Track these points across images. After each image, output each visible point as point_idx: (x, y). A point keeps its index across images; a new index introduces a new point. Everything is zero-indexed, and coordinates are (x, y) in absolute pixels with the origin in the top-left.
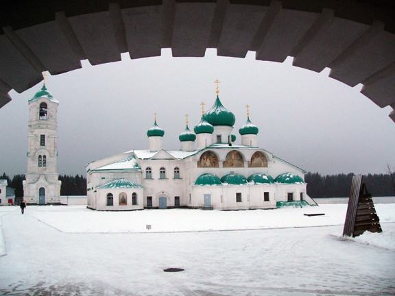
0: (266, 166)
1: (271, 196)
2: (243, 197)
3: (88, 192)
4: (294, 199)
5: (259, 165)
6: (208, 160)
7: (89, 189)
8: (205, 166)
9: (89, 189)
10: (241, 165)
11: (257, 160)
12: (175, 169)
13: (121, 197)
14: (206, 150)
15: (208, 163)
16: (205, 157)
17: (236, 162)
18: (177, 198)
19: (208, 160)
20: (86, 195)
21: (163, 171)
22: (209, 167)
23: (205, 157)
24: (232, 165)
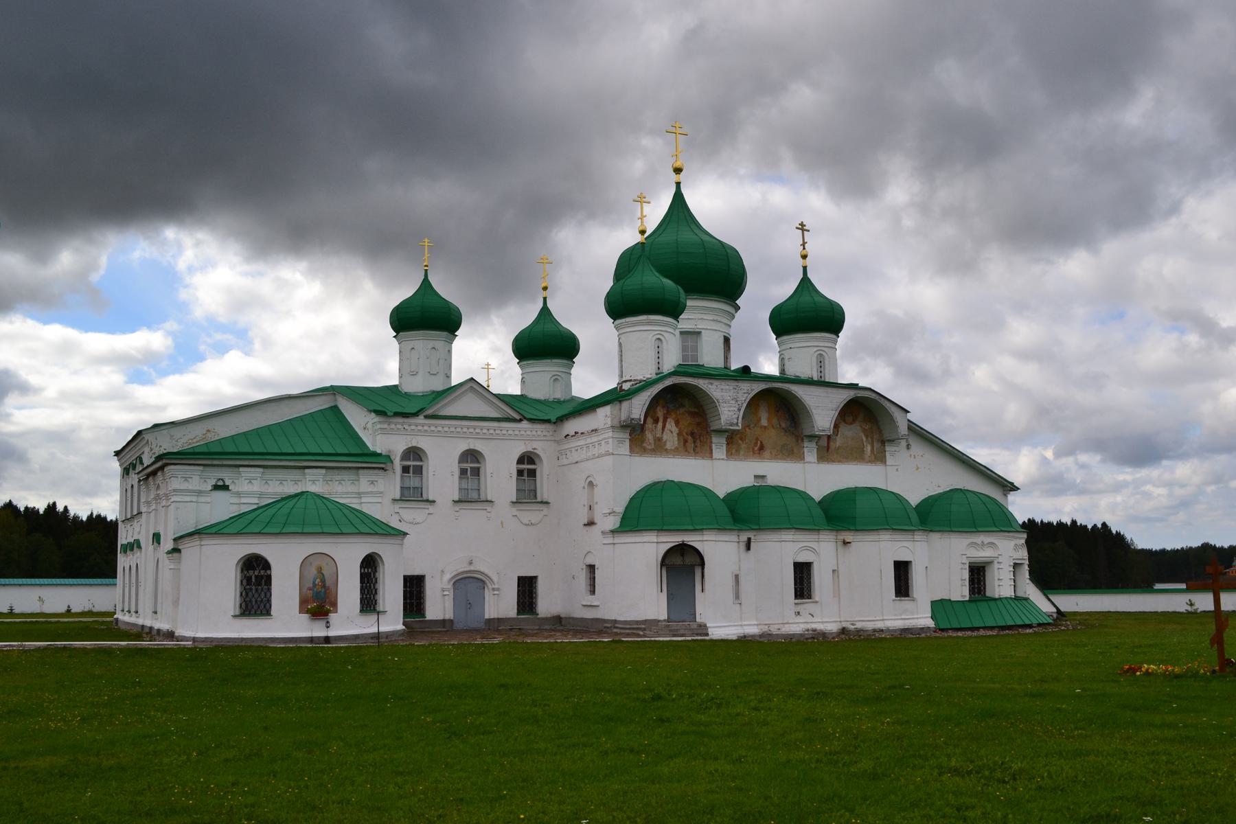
0: (880, 458)
1: (918, 578)
2: (820, 579)
3: (123, 561)
4: (989, 594)
5: (854, 455)
6: (671, 425)
7: (134, 546)
8: (659, 448)
9: (134, 546)
10: (791, 453)
11: (851, 432)
12: (521, 460)
13: (312, 572)
14: (668, 382)
15: (670, 433)
16: (660, 413)
17: (772, 436)
18: (527, 587)
19: (671, 425)
20: (112, 574)
21: (471, 463)
22: (676, 452)
23: (660, 413)
24: (759, 450)
